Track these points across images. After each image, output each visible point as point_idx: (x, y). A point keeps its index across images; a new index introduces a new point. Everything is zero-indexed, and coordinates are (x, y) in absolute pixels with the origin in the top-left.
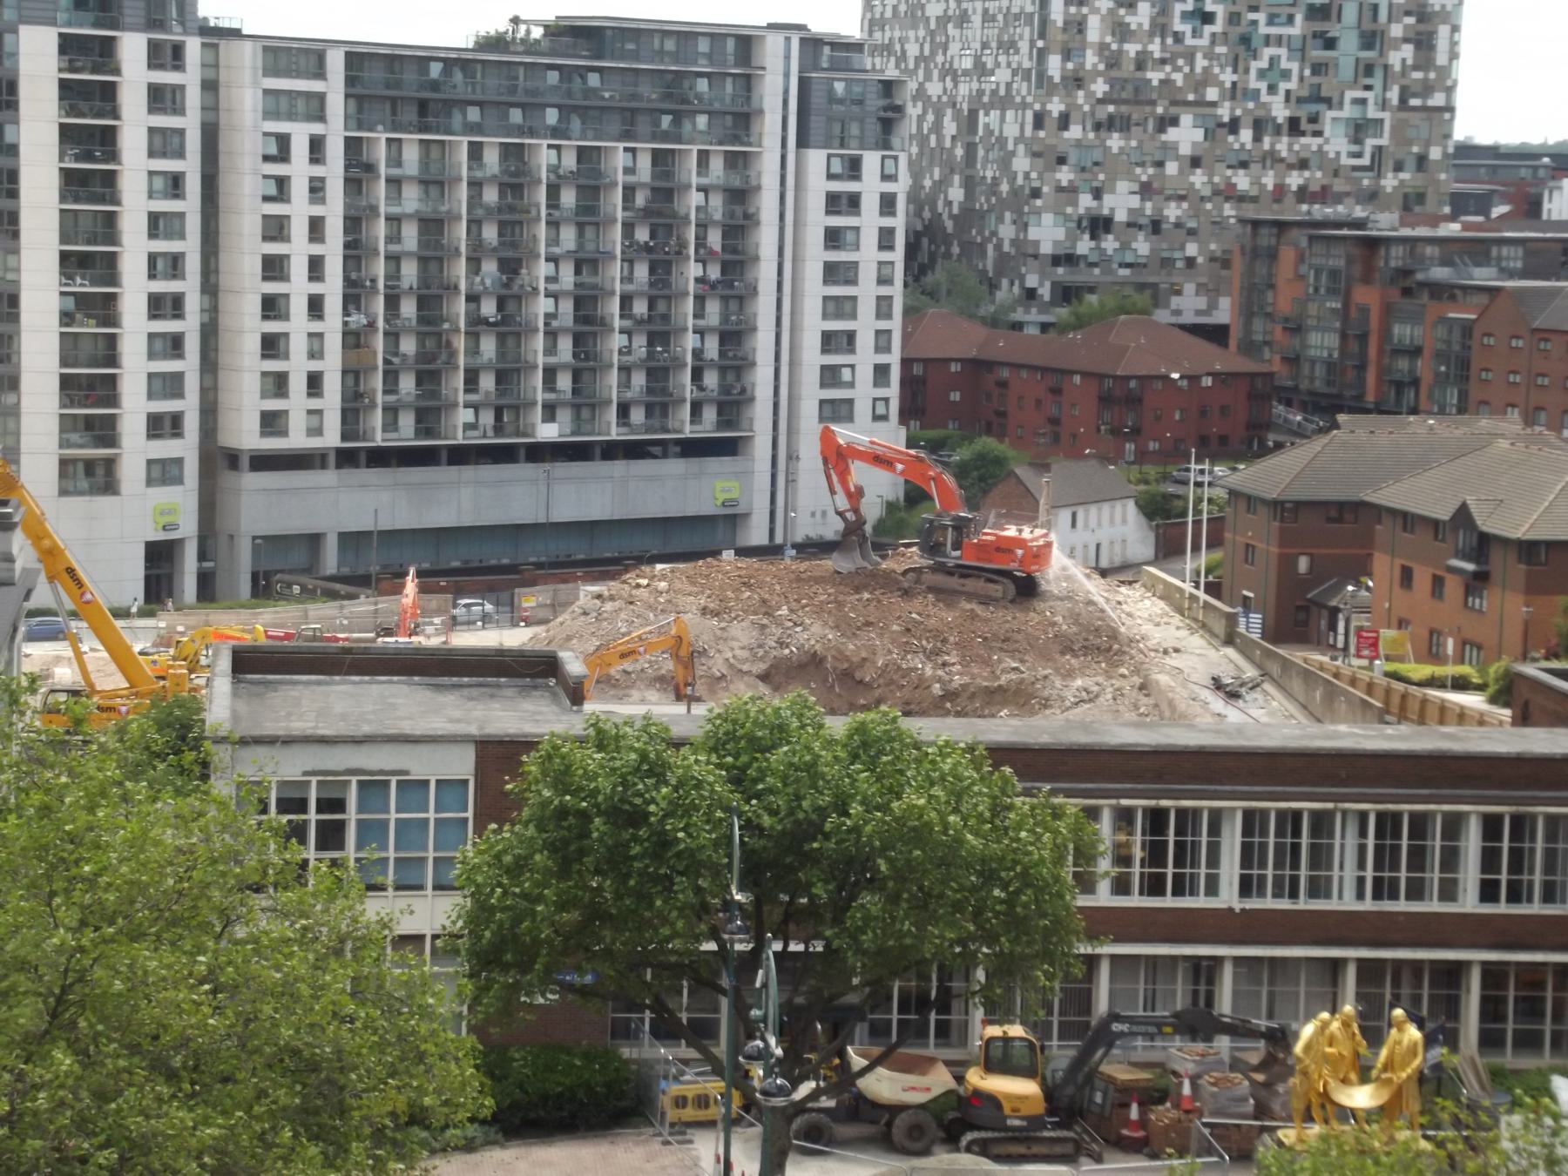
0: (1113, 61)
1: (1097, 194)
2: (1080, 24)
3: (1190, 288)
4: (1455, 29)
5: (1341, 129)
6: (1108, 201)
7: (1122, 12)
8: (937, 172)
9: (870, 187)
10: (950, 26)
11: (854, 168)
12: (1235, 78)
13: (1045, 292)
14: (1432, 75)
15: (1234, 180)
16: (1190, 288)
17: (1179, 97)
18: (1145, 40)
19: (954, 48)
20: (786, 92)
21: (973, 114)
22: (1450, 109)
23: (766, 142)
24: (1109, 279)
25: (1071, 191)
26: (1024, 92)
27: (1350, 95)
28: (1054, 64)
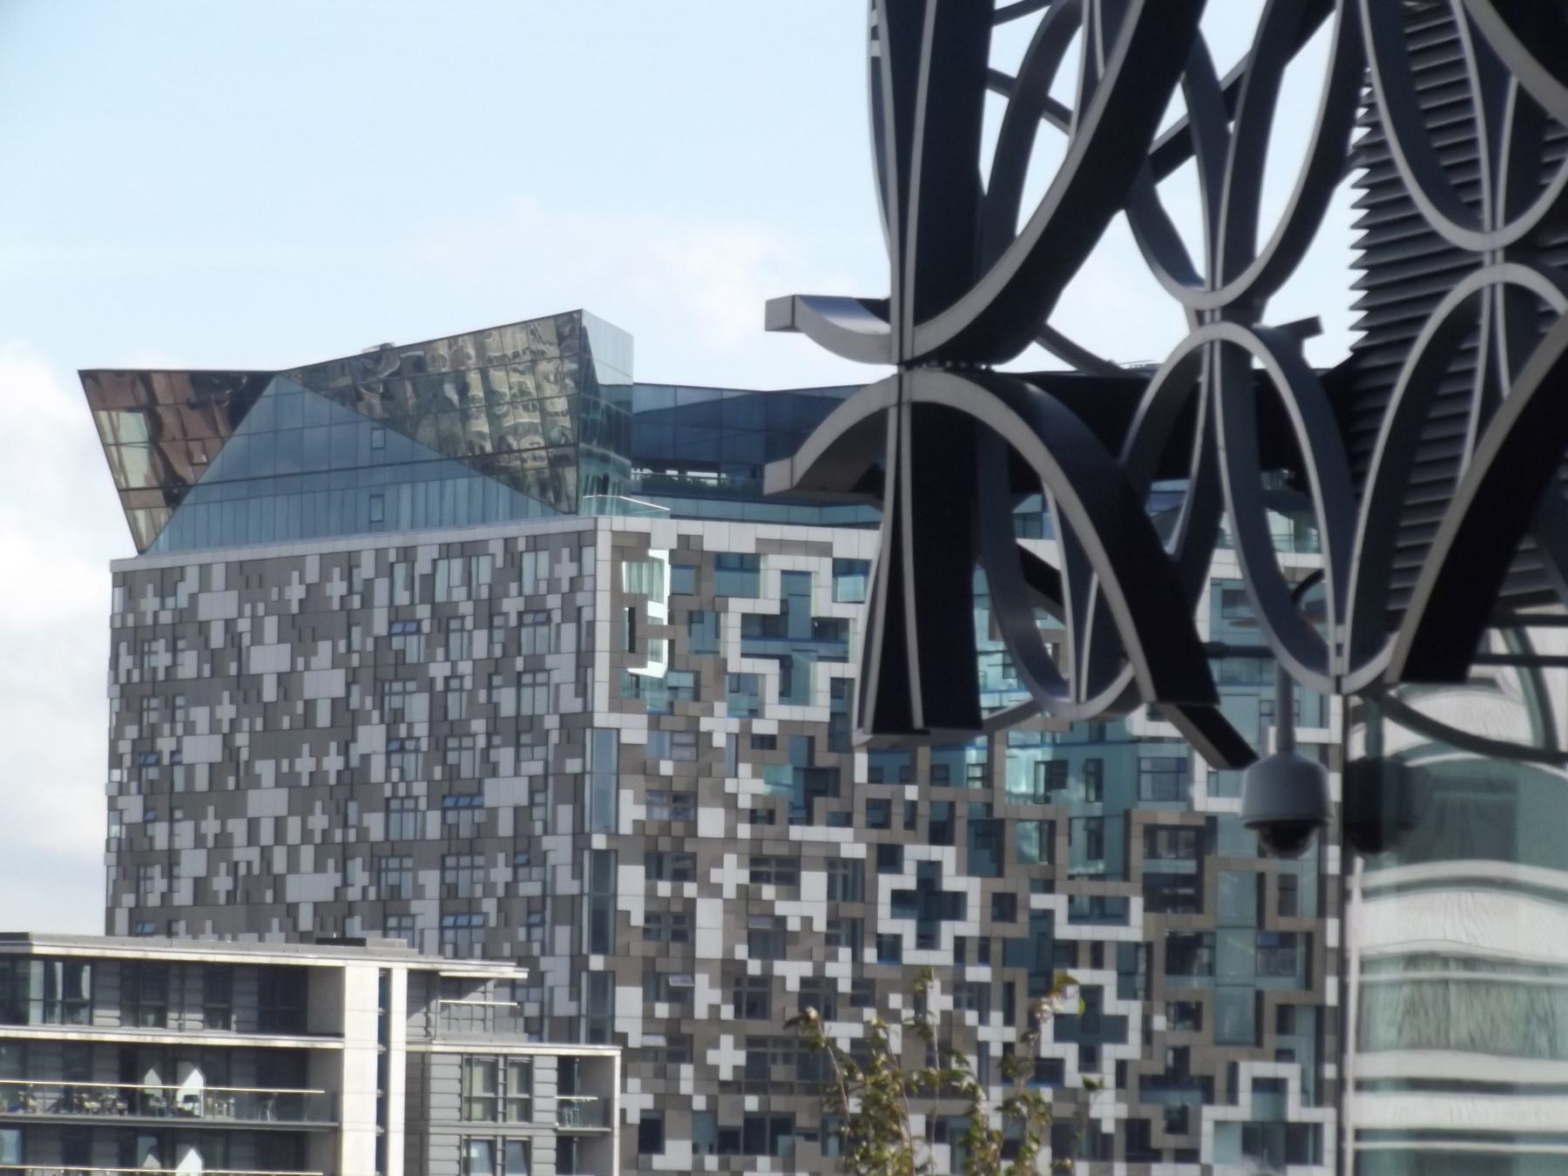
2: (678, 918)
7: (768, 892)
12: (1011, 1034)
18: (819, 951)
27: (1249, 1070)
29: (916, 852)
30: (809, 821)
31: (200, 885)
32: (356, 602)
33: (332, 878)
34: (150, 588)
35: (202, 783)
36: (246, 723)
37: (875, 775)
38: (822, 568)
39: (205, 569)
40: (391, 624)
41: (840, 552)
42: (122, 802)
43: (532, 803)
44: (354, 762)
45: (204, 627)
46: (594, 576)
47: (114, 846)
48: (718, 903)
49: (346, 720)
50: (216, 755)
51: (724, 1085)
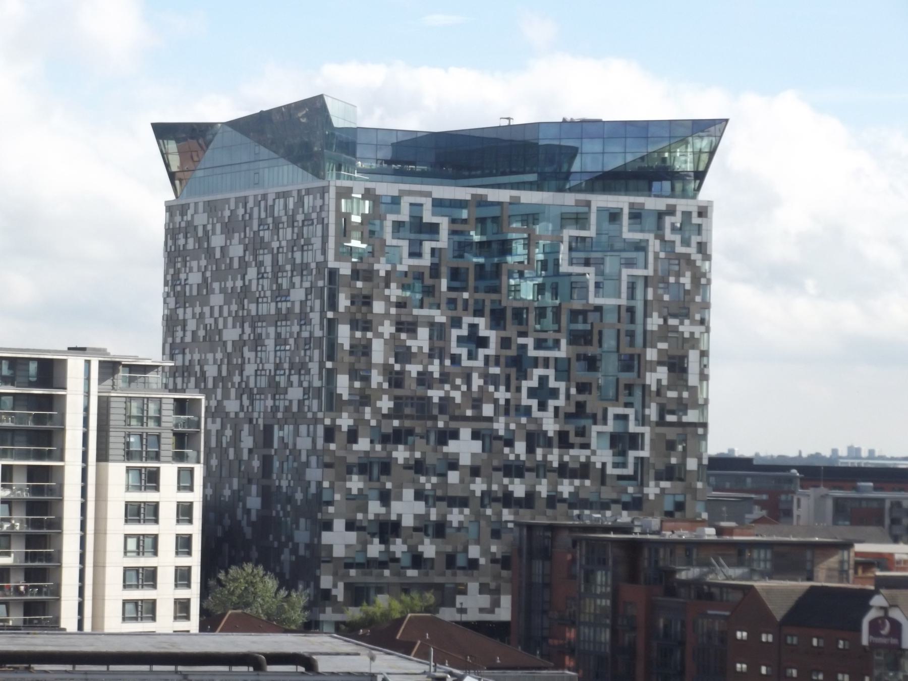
0: (396, 380)
1: (385, 498)
3: (473, 587)
4: (704, 354)
5: (607, 441)
6: (396, 507)
7: (403, 336)
8: (235, 482)
10: (246, 349)
11: (152, 479)
12: (508, 395)
13: (339, 593)
14: (685, 395)
15: (511, 488)
16: (473, 587)
17: (457, 413)
18: (426, 361)
19: (250, 369)
20: (86, 409)
21: (268, 431)
22: (704, 425)
23: (68, 455)
24: (396, 580)
25: (360, 500)
26: (315, 408)
27: (612, 411)
28: (343, 383)
29: (467, 320)
30: (421, 307)
31: (194, 333)
32: (247, 216)
33: (238, 331)
34: (178, 212)
35: (195, 293)
36: (210, 267)
37: (450, 289)
38: (427, 203)
39: (196, 204)
40: (259, 226)
41: (435, 195)
42: (168, 300)
43: (307, 299)
44: (247, 283)
45: (196, 228)
46: (329, 205)
47: (165, 319)
48: (382, 340)
49: (244, 265)
50: (200, 281)
51: (384, 416)
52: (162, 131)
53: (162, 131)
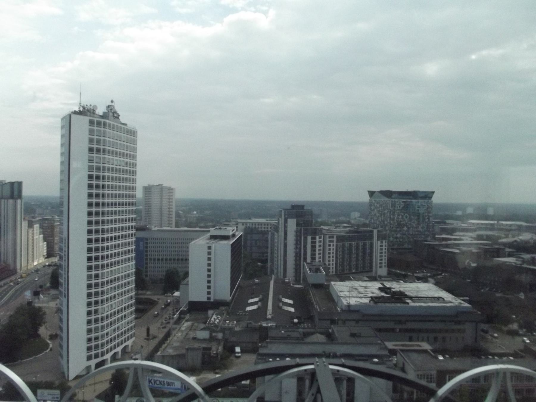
0: (397, 221)
1: (396, 235)
9: (384, 244)
52: (369, 192)
53: (369, 192)
